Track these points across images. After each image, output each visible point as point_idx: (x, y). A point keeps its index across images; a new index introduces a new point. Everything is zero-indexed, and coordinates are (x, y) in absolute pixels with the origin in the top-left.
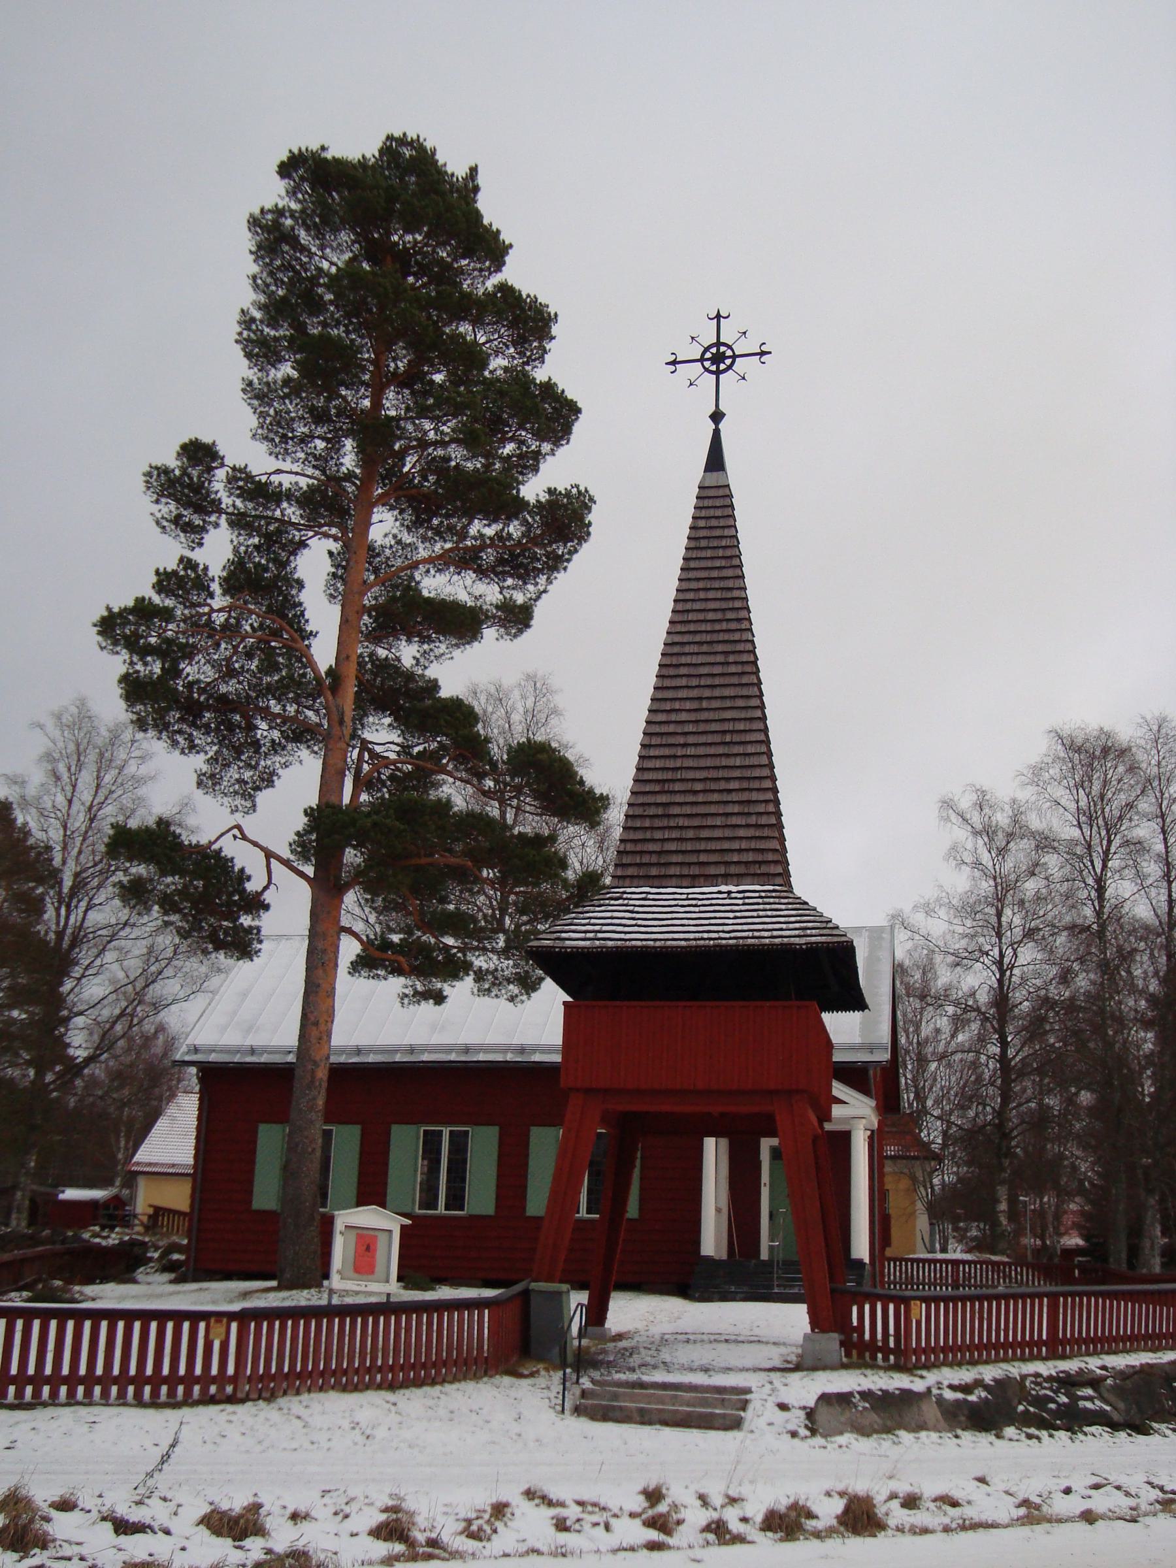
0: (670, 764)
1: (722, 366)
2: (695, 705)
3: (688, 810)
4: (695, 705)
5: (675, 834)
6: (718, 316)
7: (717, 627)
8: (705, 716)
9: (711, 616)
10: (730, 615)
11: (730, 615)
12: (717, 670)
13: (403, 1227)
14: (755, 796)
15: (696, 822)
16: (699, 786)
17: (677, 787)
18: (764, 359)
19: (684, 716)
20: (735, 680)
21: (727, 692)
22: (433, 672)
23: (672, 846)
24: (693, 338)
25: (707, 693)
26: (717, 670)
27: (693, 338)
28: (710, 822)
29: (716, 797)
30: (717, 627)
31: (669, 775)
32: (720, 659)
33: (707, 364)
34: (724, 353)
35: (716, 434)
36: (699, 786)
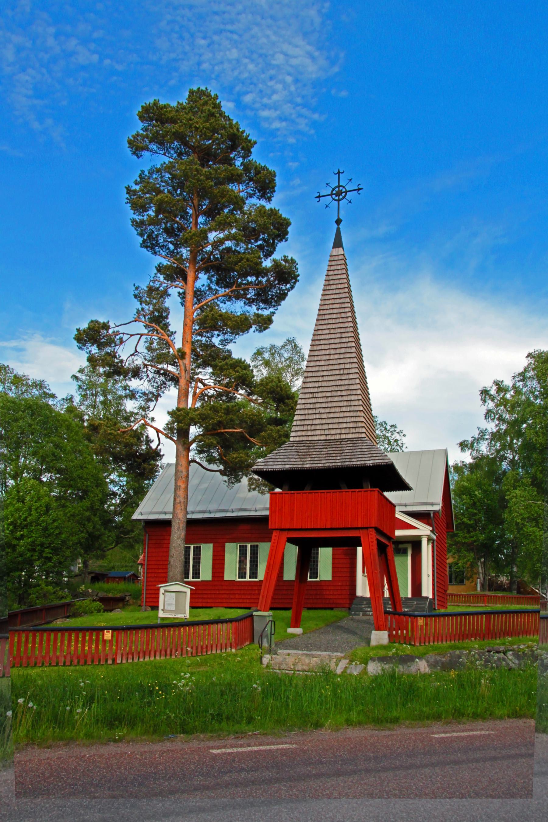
0: (317, 385)
1: (341, 197)
2: (327, 357)
3: (324, 405)
4: (327, 357)
5: (318, 416)
6: (339, 173)
7: (338, 321)
8: (331, 362)
9: (334, 316)
10: (343, 315)
11: (343, 315)
12: (337, 341)
13: (191, 589)
14: (353, 398)
15: (328, 410)
16: (329, 394)
17: (320, 395)
18: (360, 192)
19: (322, 363)
20: (345, 345)
21: (343, 351)
22: (229, 347)
23: (317, 422)
24: (327, 184)
25: (333, 352)
26: (337, 341)
27: (327, 184)
28: (333, 410)
29: (336, 399)
30: (338, 321)
31: (316, 390)
32: (338, 335)
33: (334, 196)
34: (341, 190)
35: (338, 230)
36: (329, 394)
